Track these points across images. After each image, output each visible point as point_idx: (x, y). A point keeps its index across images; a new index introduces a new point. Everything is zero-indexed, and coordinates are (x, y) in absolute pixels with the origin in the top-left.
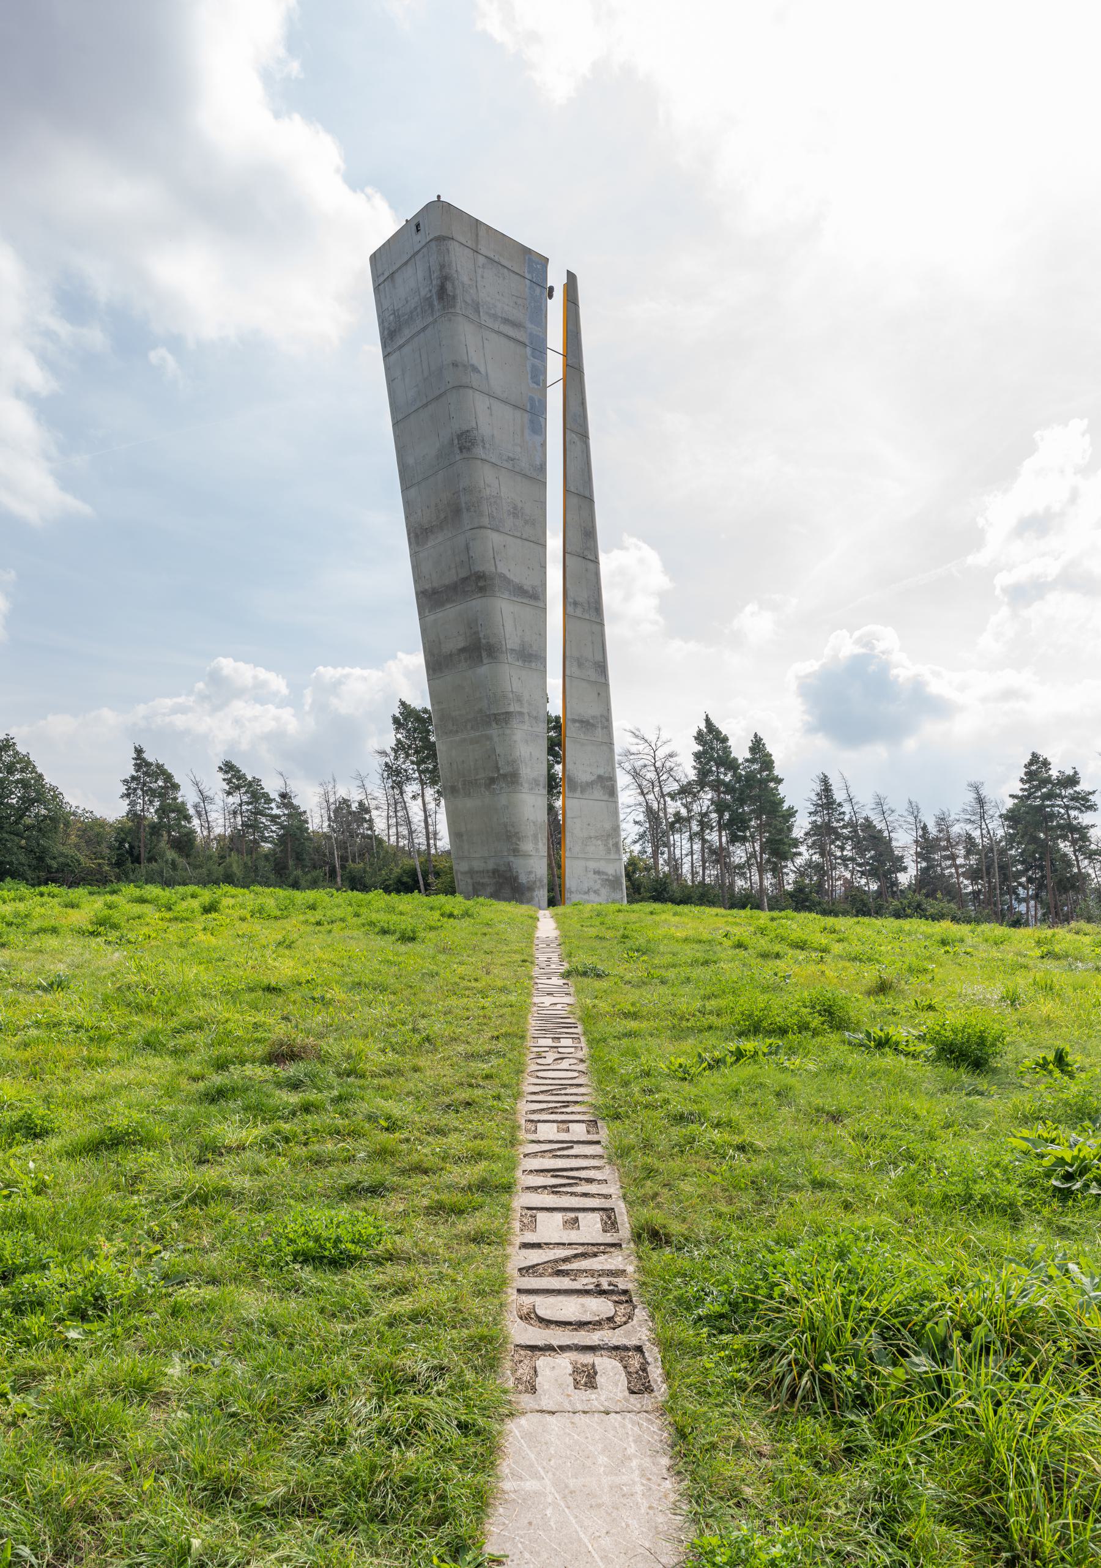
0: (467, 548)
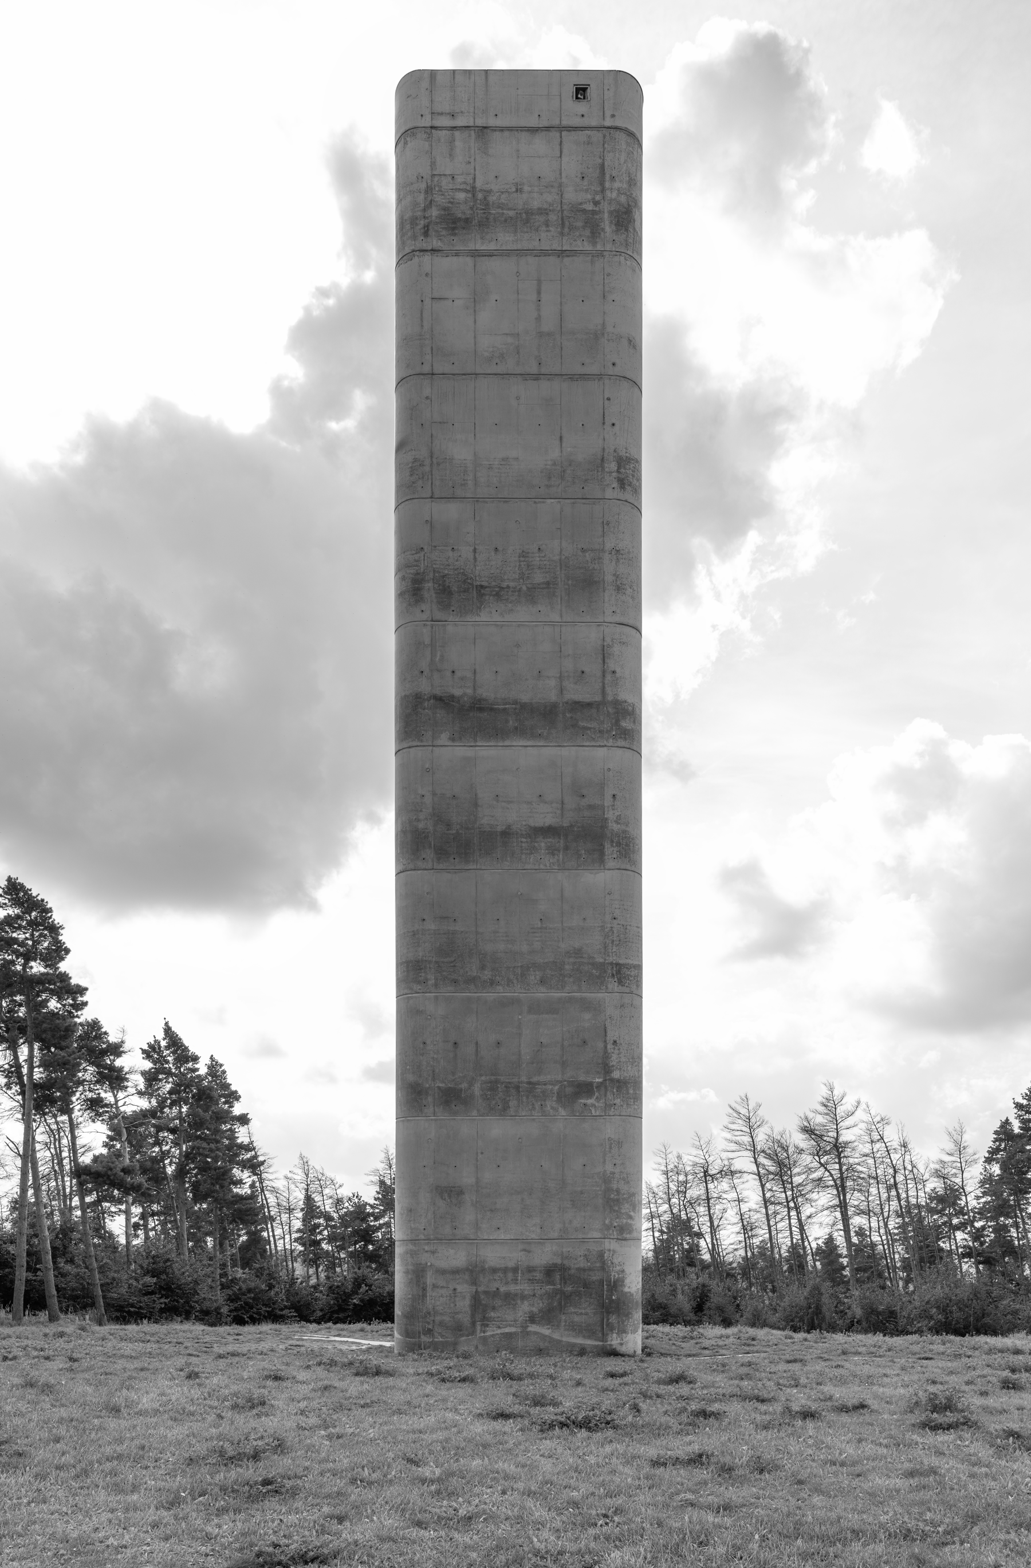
0: (604, 653)
